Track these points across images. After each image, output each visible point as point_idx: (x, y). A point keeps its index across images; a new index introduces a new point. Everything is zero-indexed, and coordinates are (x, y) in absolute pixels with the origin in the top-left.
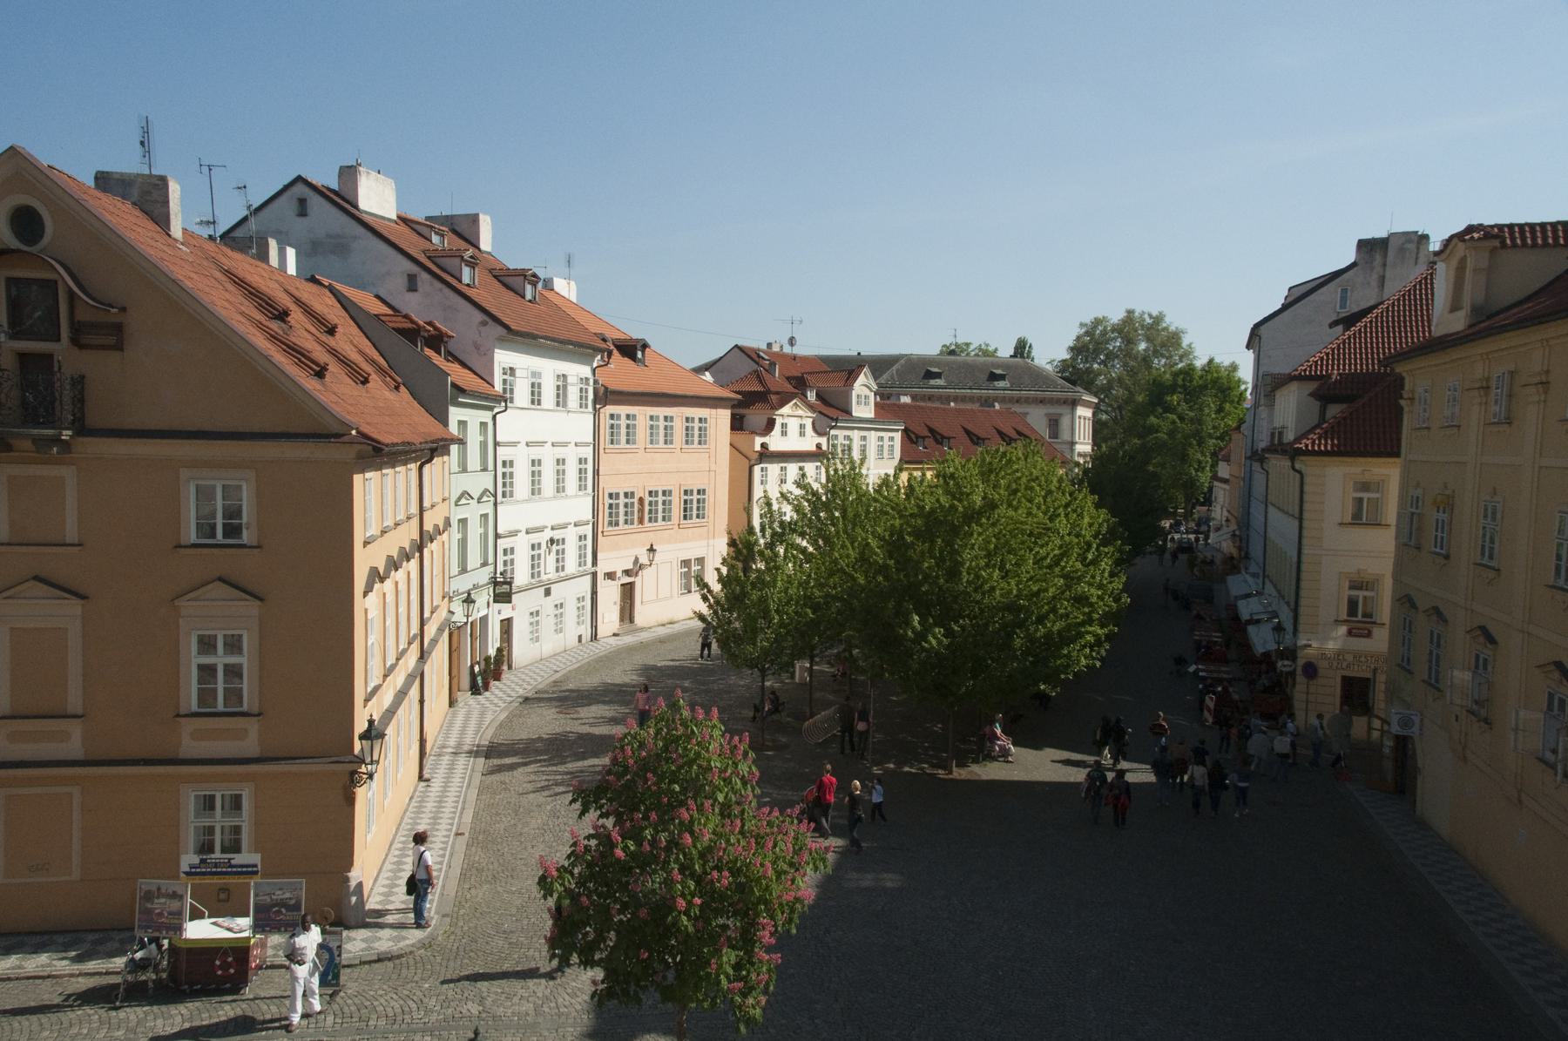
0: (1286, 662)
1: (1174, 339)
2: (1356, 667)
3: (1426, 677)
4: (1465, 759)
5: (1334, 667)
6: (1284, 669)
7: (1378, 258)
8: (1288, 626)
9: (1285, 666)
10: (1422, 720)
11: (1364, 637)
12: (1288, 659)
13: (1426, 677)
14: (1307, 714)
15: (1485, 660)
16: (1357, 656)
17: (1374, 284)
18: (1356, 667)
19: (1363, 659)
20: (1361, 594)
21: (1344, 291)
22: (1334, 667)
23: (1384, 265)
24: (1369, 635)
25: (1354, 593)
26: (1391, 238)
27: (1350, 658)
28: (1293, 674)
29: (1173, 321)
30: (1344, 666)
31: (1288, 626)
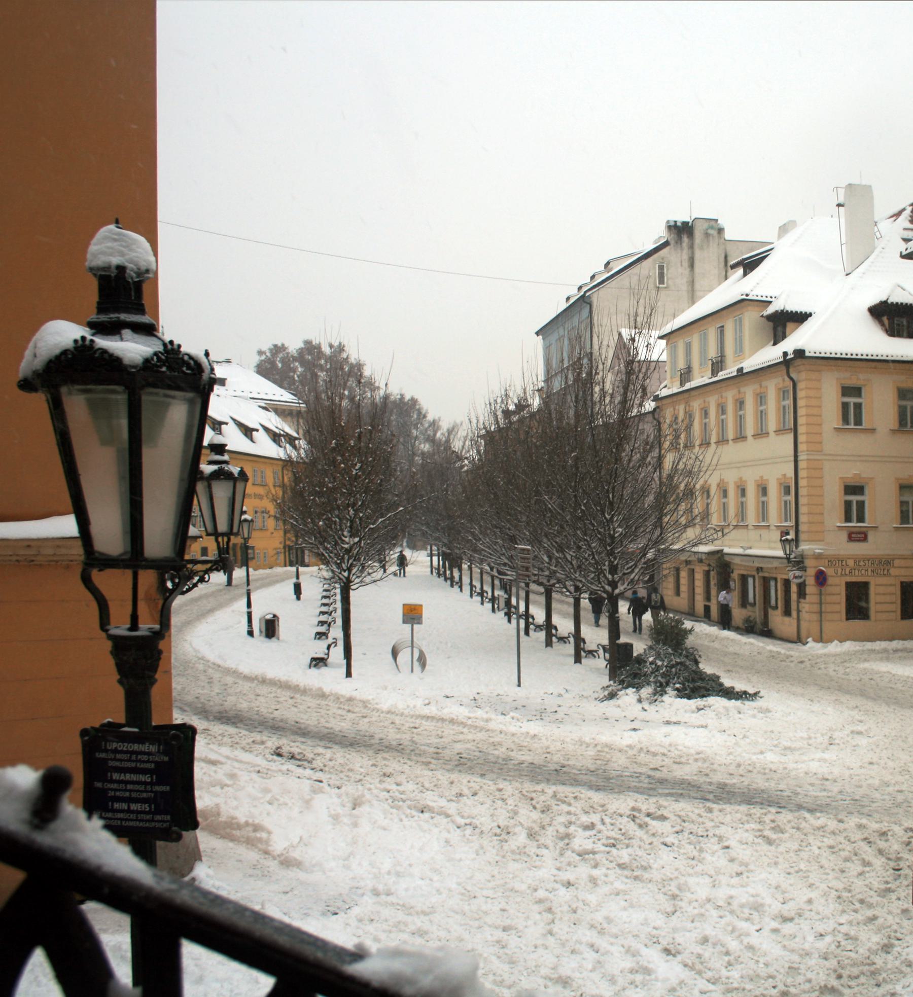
1: (356, 370)
7: (685, 239)
11: (859, 541)
16: (857, 560)
17: (686, 264)
18: (857, 571)
19: (862, 563)
20: (854, 498)
21: (661, 268)
23: (691, 247)
24: (865, 539)
25: (850, 498)
26: (697, 222)
27: (851, 563)
29: (353, 354)
30: (847, 572)
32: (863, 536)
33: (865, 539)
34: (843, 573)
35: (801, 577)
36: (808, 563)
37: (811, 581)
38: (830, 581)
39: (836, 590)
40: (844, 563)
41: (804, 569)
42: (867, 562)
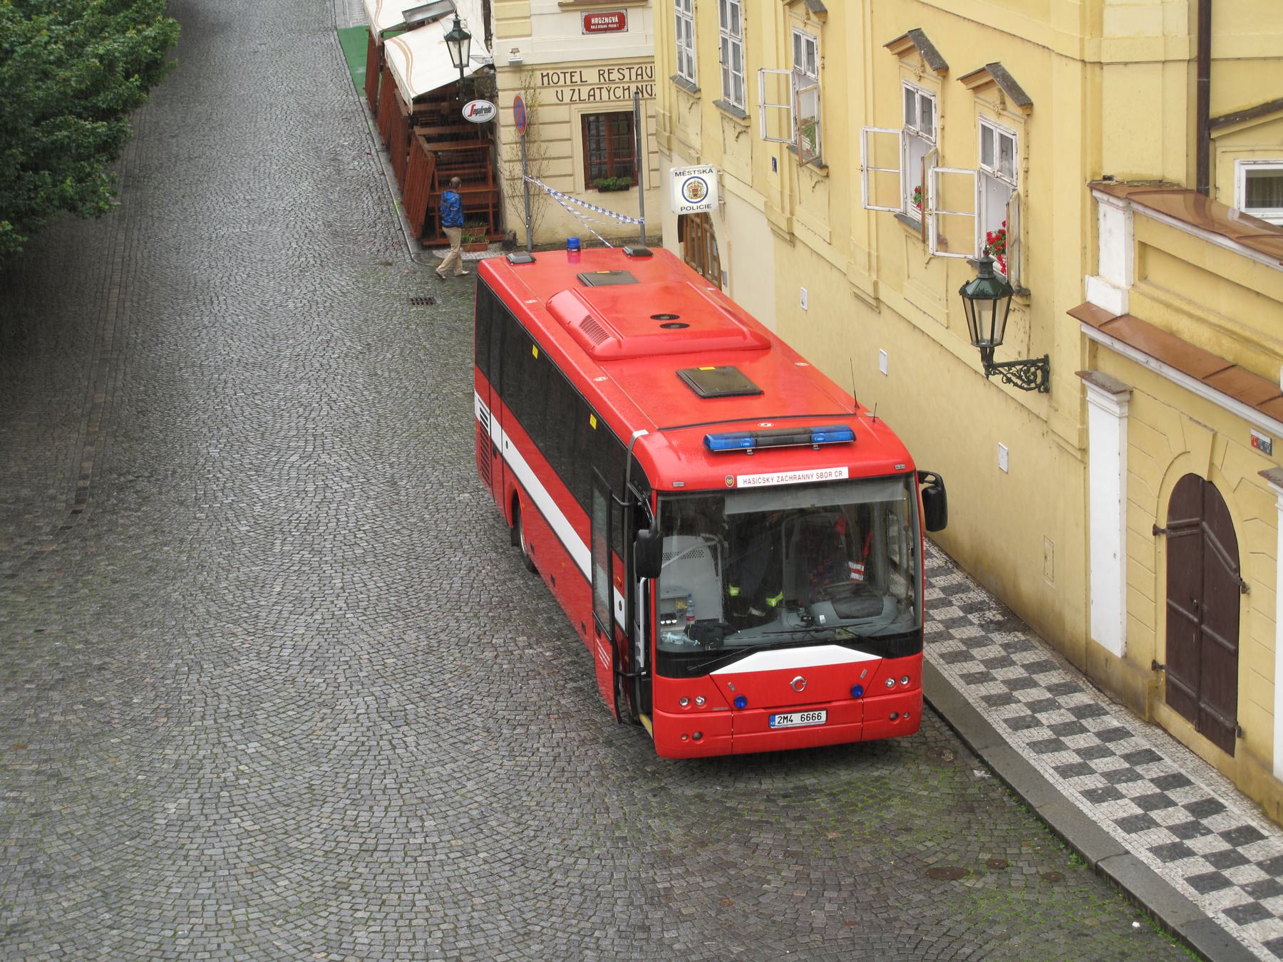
0: (480, 104)
2: (604, 92)
3: (720, 96)
4: (791, 239)
5: (567, 99)
6: (476, 119)
8: (474, 25)
9: (474, 112)
10: (721, 183)
12: (482, 97)
13: (720, 96)
14: (528, 207)
15: (810, 44)
16: (605, 68)
18: (604, 92)
19: (615, 76)
22: (567, 99)
24: (621, 25)
27: (591, 76)
28: (491, 127)
30: (584, 96)
31: (474, 25)
32: (616, 19)
33: (621, 25)
34: (576, 97)
35: (488, 110)
36: (503, 81)
37: (507, 117)
38: (545, 114)
39: (562, 131)
40: (576, 78)
41: (491, 95)
42: (626, 72)
